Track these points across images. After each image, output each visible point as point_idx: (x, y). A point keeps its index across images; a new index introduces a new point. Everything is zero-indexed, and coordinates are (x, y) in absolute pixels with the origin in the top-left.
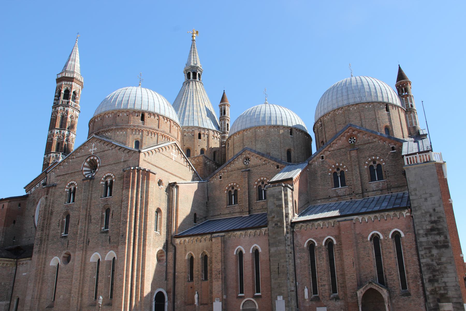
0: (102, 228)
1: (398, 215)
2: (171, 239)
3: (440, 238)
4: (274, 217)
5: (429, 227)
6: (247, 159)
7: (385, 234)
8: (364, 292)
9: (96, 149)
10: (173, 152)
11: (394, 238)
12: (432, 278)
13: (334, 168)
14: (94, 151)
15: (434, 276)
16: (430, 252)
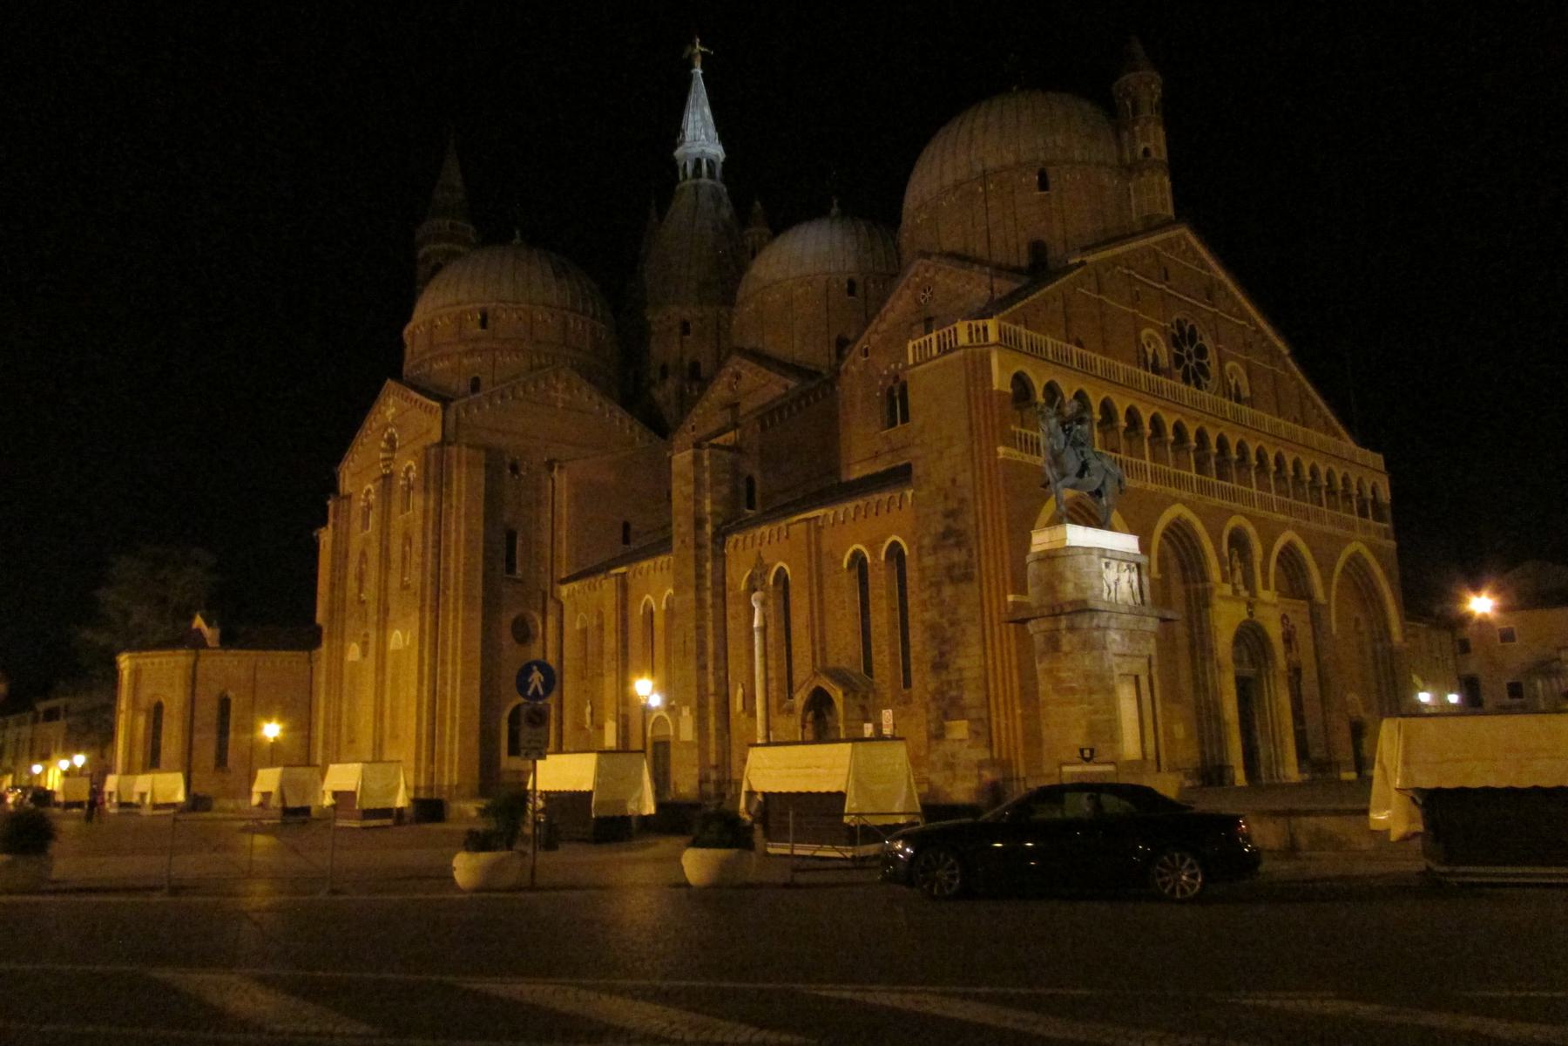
0: (406, 579)
1: (898, 500)
2: (552, 586)
3: (958, 556)
4: (679, 526)
5: (941, 529)
6: (738, 376)
7: (873, 546)
8: (806, 696)
9: (393, 410)
10: (556, 390)
11: (895, 560)
12: (938, 659)
13: (888, 376)
14: (393, 414)
15: (942, 654)
16: (939, 592)
